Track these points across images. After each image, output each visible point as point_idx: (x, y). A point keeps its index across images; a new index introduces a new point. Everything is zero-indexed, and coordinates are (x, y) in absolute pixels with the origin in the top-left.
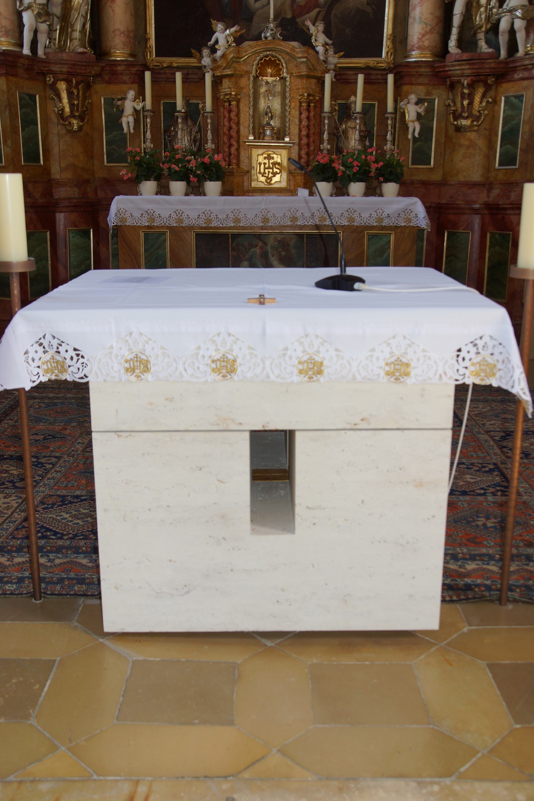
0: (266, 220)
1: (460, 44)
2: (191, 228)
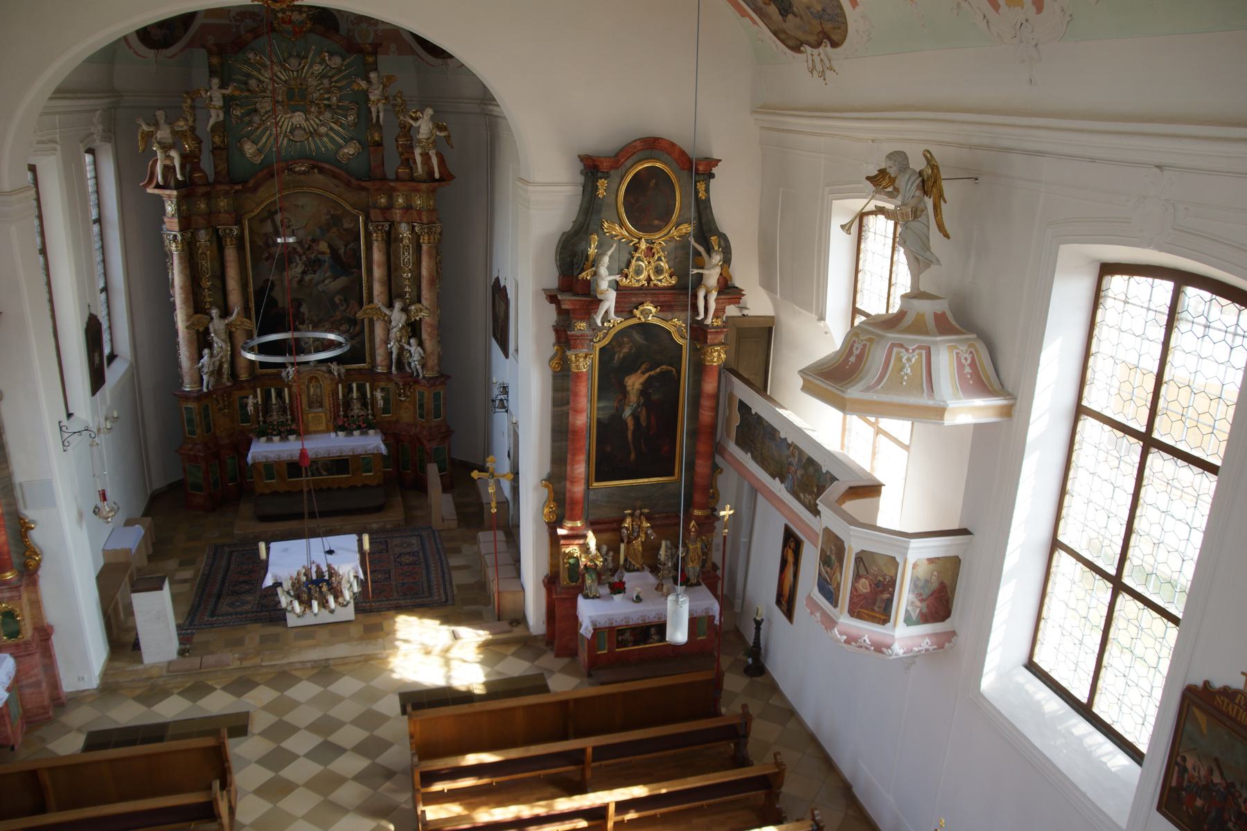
0: (317, 455)
2: (284, 461)
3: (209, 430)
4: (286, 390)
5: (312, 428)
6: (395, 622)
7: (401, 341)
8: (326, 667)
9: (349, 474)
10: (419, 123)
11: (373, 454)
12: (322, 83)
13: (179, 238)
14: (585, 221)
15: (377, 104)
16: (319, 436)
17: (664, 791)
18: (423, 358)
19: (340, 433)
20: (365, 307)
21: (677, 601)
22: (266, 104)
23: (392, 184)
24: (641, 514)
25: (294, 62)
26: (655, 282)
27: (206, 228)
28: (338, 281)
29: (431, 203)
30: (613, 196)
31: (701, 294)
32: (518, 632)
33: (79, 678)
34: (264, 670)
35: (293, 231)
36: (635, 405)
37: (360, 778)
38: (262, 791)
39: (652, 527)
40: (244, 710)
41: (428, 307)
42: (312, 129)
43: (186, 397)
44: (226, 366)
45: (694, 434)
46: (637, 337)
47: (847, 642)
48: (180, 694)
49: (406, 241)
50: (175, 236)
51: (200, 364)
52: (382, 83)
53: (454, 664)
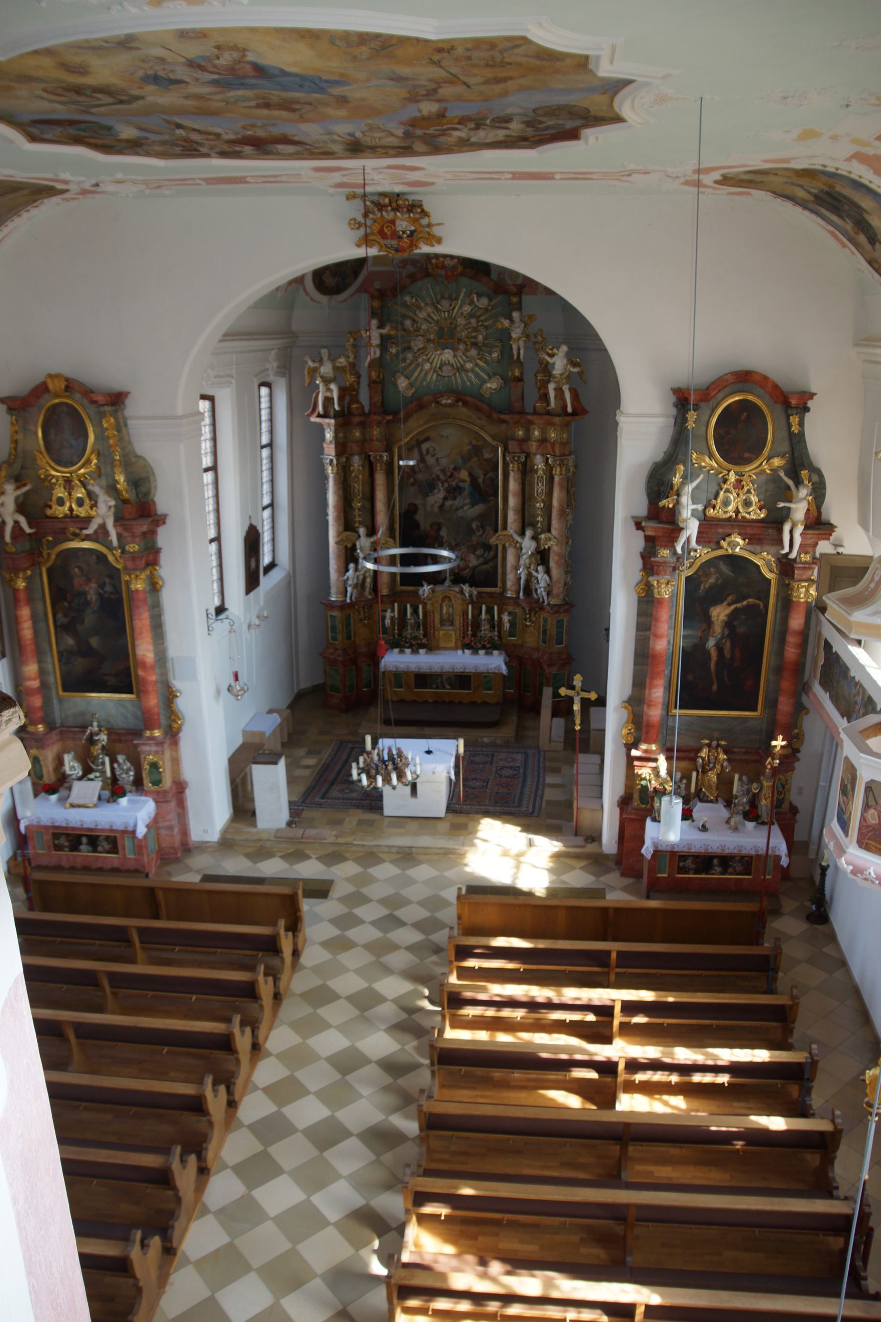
1: (524, 593)
2: (413, 672)
3: (349, 637)
4: (421, 607)
5: (442, 644)
6: (479, 823)
7: (529, 568)
8: (409, 854)
9: (470, 689)
10: (554, 359)
11: (494, 673)
12: (470, 323)
13: (335, 462)
14: (675, 451)
15: (518, 341)
16: (447, 652)
17: (671, 999)
18: (549, 585)
19: (467, 651)
20: (500, 533)
21: (671, 801)
22: (420, 342)
23: (529, 417)
24: (718, 746)
25: (445, 303)
26: (744, 514)
27: (360, 454)
28: (475, 507)
29: (565, 436)
30: (703, 429)
31: (787, 528)
32: (591, 848)
33: (204, 830)
34: (354, 849)
35: (437, 460)
36: (719, 636)
37: (411, 948)
38: (326, 944)
39: (729, 760)
40: (331, 878)
41: (557, 536)
42: (459, 365)
43: (331, 606)
44: (368, 580)
45: (779, 670)
46: (724, 568)
47: (854, 872)
48: (282, 857)
49: (540, 472)
50: (331, 460)
51: (346, 577)
52: (524, 322)
53: (523, 867)
